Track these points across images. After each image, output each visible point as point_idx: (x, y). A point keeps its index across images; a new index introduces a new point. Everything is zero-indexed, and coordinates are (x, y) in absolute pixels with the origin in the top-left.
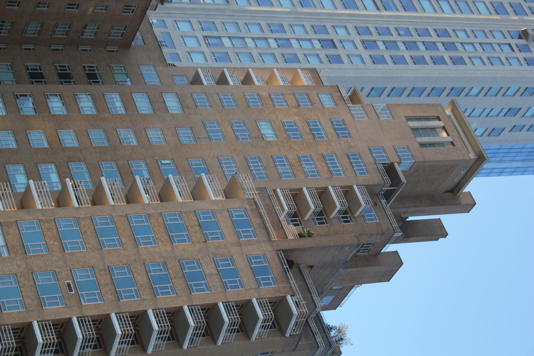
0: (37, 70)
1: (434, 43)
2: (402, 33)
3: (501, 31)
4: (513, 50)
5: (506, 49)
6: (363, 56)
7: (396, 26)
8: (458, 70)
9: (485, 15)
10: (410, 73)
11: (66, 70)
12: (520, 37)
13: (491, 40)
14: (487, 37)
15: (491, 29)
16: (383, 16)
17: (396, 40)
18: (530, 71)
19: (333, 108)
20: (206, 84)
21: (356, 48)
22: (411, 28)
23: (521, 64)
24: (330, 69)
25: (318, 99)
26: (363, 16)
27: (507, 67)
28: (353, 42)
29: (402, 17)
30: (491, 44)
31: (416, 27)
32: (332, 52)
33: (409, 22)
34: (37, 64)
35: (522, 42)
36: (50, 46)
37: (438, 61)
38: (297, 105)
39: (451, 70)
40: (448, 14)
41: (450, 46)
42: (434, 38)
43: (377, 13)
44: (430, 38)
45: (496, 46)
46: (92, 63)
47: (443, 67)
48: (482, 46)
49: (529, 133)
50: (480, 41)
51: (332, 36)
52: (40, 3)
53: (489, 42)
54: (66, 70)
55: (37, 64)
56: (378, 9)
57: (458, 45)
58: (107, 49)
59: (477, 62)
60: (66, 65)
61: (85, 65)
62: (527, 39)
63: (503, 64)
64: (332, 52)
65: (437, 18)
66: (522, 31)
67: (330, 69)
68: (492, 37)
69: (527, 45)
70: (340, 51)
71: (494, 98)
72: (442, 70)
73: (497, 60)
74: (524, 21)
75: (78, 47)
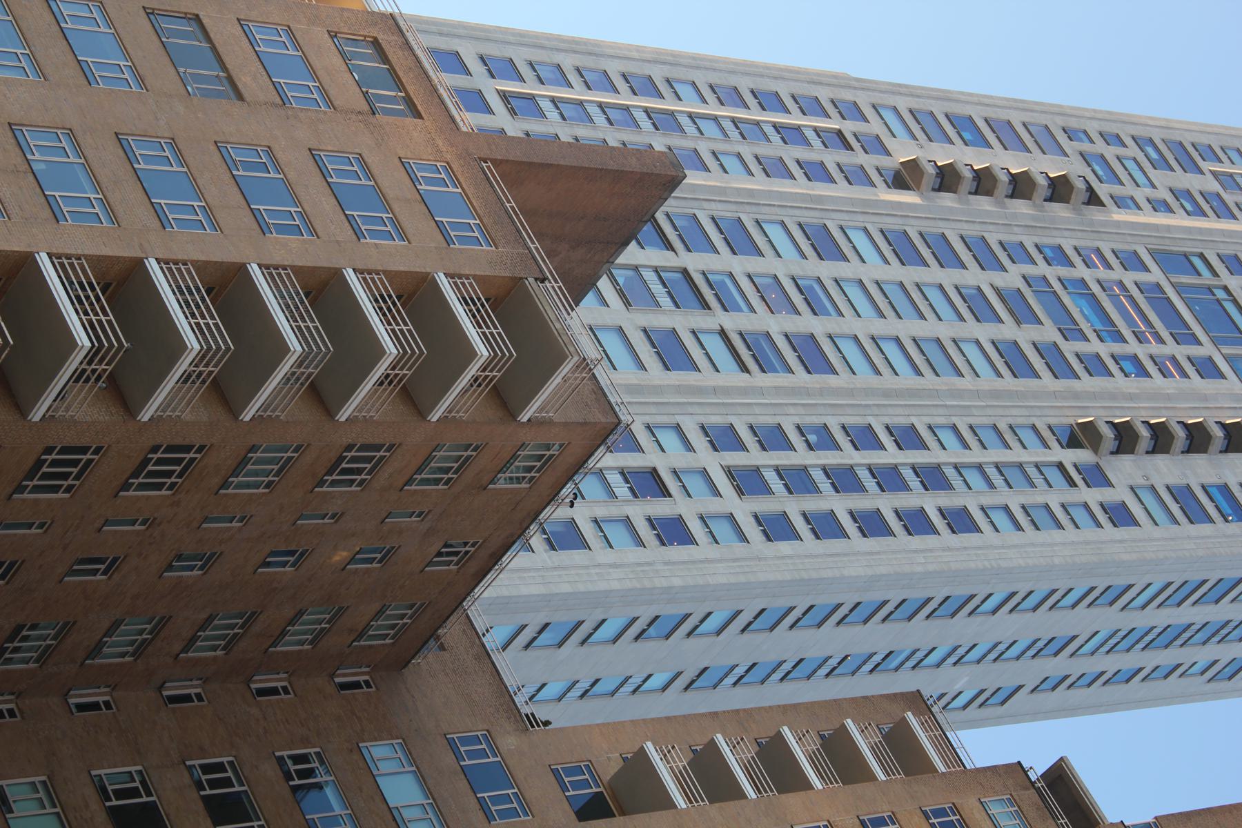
0: (134, 793)
1: (895, 468)
2: (812, 438)
3: (1034, 427)
4: (1072, 483)
5: (1054, 476)
6: (739, 517)
7: (797, 420)
8: (965, 548)
9: (987, 380)
10: (856, 563)
11: (227, 783)
12: (1073, 442)
13: (1016, 455)
14: (1008, 446)
15: (1011, 421)
16: (761, 391)
17: (807, 462)
18: (1121, 542)
20: (684, 806)
21: (716, 493)
22: (834, 425)
23: (1099, 525)
24: (666, 563)
26: (715, 391)
27: (1070, 533)
28: (704, 473)
29: (807, 392)
30: (1020, 466)
32: (661, 508)
33: (824, 405)
34: (133, 769)
35: (1084, 456)
36: (161, 688)
37: (916, 523)
39: (949, 549)
40: (907, 378)
41: (933, 478)
42: (890, 455)
43: (741, 379)
44: (882, 452)
45: (1032, 471)
46: (306, 742)
47: (929, 540)
50: (996, 459)
51: (650, 458)
52: (179, 557)
53: (1015, 459)
54: (227, 783)
55: (133, 769)
56: (744, 369)
57: (950, 473)
58: (337, 680)
59: (1000, 519)
60: (225, 760)
61: (285, 753)
62: (1096, 450)
63: (1060, 526)
64: (661, 508)
65: (887, 394)
66: (1078, 424)
67: (666, 563)
68: (1018, 444)
69: (1098, 466)
70: (677, 506)
71: (1030, 614)
72: (931, 551)
74: (1076, 396)
75: (249, 681)
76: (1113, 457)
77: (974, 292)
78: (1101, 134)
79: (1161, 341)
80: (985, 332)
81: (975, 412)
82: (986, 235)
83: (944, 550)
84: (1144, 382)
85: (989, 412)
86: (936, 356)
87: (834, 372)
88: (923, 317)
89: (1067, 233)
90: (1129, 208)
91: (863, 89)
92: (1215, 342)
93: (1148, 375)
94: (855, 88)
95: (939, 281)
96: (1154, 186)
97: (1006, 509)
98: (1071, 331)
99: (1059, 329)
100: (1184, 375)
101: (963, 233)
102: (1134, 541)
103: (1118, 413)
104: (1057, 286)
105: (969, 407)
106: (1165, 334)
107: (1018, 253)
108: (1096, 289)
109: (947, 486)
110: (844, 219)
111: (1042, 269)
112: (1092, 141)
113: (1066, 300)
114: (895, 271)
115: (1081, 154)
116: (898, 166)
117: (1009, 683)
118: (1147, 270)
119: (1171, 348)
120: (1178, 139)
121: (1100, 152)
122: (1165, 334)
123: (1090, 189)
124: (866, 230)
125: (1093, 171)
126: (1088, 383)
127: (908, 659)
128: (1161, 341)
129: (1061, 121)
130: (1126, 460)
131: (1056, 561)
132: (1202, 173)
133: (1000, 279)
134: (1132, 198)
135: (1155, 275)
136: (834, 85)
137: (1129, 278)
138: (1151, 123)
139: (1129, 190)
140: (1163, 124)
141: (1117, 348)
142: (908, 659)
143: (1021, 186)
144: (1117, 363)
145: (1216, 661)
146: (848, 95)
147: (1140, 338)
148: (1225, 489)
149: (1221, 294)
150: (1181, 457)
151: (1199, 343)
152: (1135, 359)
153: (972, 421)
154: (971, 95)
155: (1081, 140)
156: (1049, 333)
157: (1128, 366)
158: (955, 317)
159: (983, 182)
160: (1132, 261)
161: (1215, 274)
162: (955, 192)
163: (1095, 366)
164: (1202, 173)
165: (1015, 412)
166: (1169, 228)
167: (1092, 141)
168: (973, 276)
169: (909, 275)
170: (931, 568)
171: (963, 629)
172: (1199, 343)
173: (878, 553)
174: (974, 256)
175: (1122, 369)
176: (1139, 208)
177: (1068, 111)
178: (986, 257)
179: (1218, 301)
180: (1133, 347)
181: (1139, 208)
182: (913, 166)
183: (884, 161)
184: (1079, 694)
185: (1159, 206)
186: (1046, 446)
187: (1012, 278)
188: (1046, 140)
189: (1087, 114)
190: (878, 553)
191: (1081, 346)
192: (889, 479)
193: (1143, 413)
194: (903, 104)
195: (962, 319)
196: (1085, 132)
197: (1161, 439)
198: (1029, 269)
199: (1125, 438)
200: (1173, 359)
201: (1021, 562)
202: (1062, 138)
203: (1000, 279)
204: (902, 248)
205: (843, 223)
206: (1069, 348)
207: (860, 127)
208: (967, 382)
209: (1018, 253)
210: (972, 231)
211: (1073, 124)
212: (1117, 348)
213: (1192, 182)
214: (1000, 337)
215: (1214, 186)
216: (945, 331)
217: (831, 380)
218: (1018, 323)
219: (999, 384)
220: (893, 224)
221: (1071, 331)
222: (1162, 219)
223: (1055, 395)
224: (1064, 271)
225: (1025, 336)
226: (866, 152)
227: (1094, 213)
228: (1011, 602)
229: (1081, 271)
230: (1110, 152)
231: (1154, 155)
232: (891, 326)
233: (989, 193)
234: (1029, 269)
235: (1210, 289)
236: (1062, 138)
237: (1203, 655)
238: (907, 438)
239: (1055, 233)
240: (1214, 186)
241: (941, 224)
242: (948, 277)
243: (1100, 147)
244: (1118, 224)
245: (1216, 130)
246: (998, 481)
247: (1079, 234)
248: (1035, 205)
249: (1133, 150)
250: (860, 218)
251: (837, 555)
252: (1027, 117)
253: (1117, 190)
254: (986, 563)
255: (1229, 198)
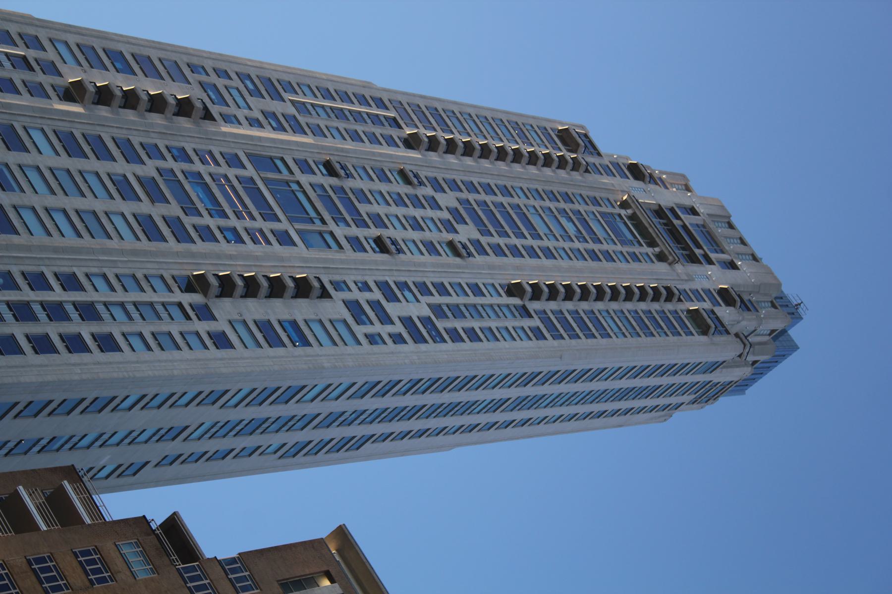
4: (188, 318)
5: (176, 312)
8: (110, 363)
9: (129, 242)
14: (143, 290)
15: (145, 272)
19: (152, 579)
22: (16, 271)
23: (206, 347)
25: (121, 559)
27: (186, 353)
30: (151, 304)
31: (23, 268)
33: (9, 257)
35: (196, 298)
37: (75, 344)
38: (87, 583)
39: (99, 363)
40: (70, 239)
41: (88, 312)
42: (57, 295)
44: (51, 293)
45: (160, 308)
47: (85, 357)
48: (138, 310)
49: (184, 466)
53: (149, 300)
57: (101, 308)
59: (136, 342)
62: (205, 294)
63: (178, 348)
65: (56, 250)
66: (193, 276)
68: (150, 289)
69: (206, 306)
72: (85, 364)
73: (168, 337)
74: (193, 255)
76: (217, 300)
77: (121, 178)
78: (214, 70)
79: (253, 218)
80: (128, 208)
81: (120, 265)
82: (130, 138)
83: (94, 364)
84: (241, 247)
85: (130, 265)
86: (93, 224)
87: (17, 233)
88: (83, 195)
89: (188, 139)
90: (233, 123)
91: (43, 27)
92: (291, 220)
93: (243, 242)
94: (37, 26)
95: (96, 169)
96: (250, 109)
97: (141, 335)
98: (190, 209)
99: (182, 208)
100: (268, 242)
101: (114, 135)
102: (230, 359)
103: (221, 268)
104: (181, 177)
105: (116, 261)
106: (255, 213)
107: (154, 152)
108: (208, 180)
109: (98, 318)
110: (27, 122)
111: (170, 163)
112: (208, 74)
113: (187, 187)
114: (65, 161)
115: (200, 83)
116: (68, 85)
117: (139, 460)
118: (244, 167)
119: (260, 223)
120: (268, 76)
121: (214, 82)
122: (255, 213)
123: (206, 108)
124: (42, 130)
125: (208, 95)
126: (201, 246)
127: (66, 442)
128: (253, 218)
129: (186, 59)
130: (226, 302)
131: (176, 372)
132: (284, 101)
133: (140, 170)
134: (235, 116)
135: (250, 171)
136: (21, 23)
137: (232, 173)
138: (249, 63)
139: (232, 110)
140: (258, 65)
141: (222, 222)
142: (66, 442)
143: (157, 104)
144: (222, 233)
145: (285, 444)
146: (31, 31)
147: (238, 216)
148: (294, 324)
149: (295, 187)
150: (264, 300)
151: (279, 220)
152: (234, 230)
153: (119, 271)
154: (121, 36)
155: (199, 73)
156: (174, 209)
157: (229, 235)
158: (107, 196)
159: (130, 100)
160: (234, 161)
161: (291, 172)
162: (109, 106)
163: (206, 234)
164: (284, 101)
165: (149, 266)
166: (260, 139)
167: (208, 74)
168: (121, 167)
169: (75, 164)
170: (84, 377)
171: (107, 421)
172: (279, 220)
173: (46, 366)
174: (122, 152)
175: (225, 237)
176: (240, 124)
177: (192, 52)
178: (131, 154)
179: (293, 191)
180: (233, 222)
181: (240, 124)
182: (79, 85)
183: (57, 81)
184: (189, 468)
185: (254, 123)
186: (171, 291)
187: (149, 169)
188: (175, 72)
189: (205, 55)
190: (46, 366)
191: (196, 220)
192: (56, 312)
193: (239, 269)
194: (72, 40)
195: (112, 197)
196: (203, 68)
197: (251, 288)
198: (161, 164)
199: (226, 287)
200: (261, 231)
201: (150, 373)
202: (187, 72)
203: (140, 170)
204: (69, 144)
205: (26, 124)
206: (188, 221)
207: (40, 54)
208: (115, 243)
209: (154, 152)
210: (120, 134)
211: (195, 61)
212: (222, 222)
213: (276, 107)
214: (139, 211)
215: (292, 111)
216: (99, 206)
217: (15, 239)
218: (153, 202)
219: (138, 245)
220: (63, 127)
221: (190, 209)
222: (255, 132)
223: (177, 254)
224: (186, 166)
225: (157, 211)
226: (44, 73)
227: (208, 126)
228: (142, 402)
229: (198, 167)
230: (220, 83)
231: (251, 86)
232: (59, 201)
233: (134, 107)
234: (161, 164)
235: (287, 183)
236: (187, 72)
237: (276, 440)
238: (70, 282)
239: (181, 138)
240: (292, 111)
241: (98, 128)
242: (103, 167)
243: (213, 79)
244: (225, 134)
245: (294, 71)
246: (135, 315)
247: (197, 140)
248: (166, 118)
249: (236, 82)
250: (39, 121)
251: (16, 367)
252: (162, 55)
253: (224, 109)
254: (125, 374)
255: (302, 119)
